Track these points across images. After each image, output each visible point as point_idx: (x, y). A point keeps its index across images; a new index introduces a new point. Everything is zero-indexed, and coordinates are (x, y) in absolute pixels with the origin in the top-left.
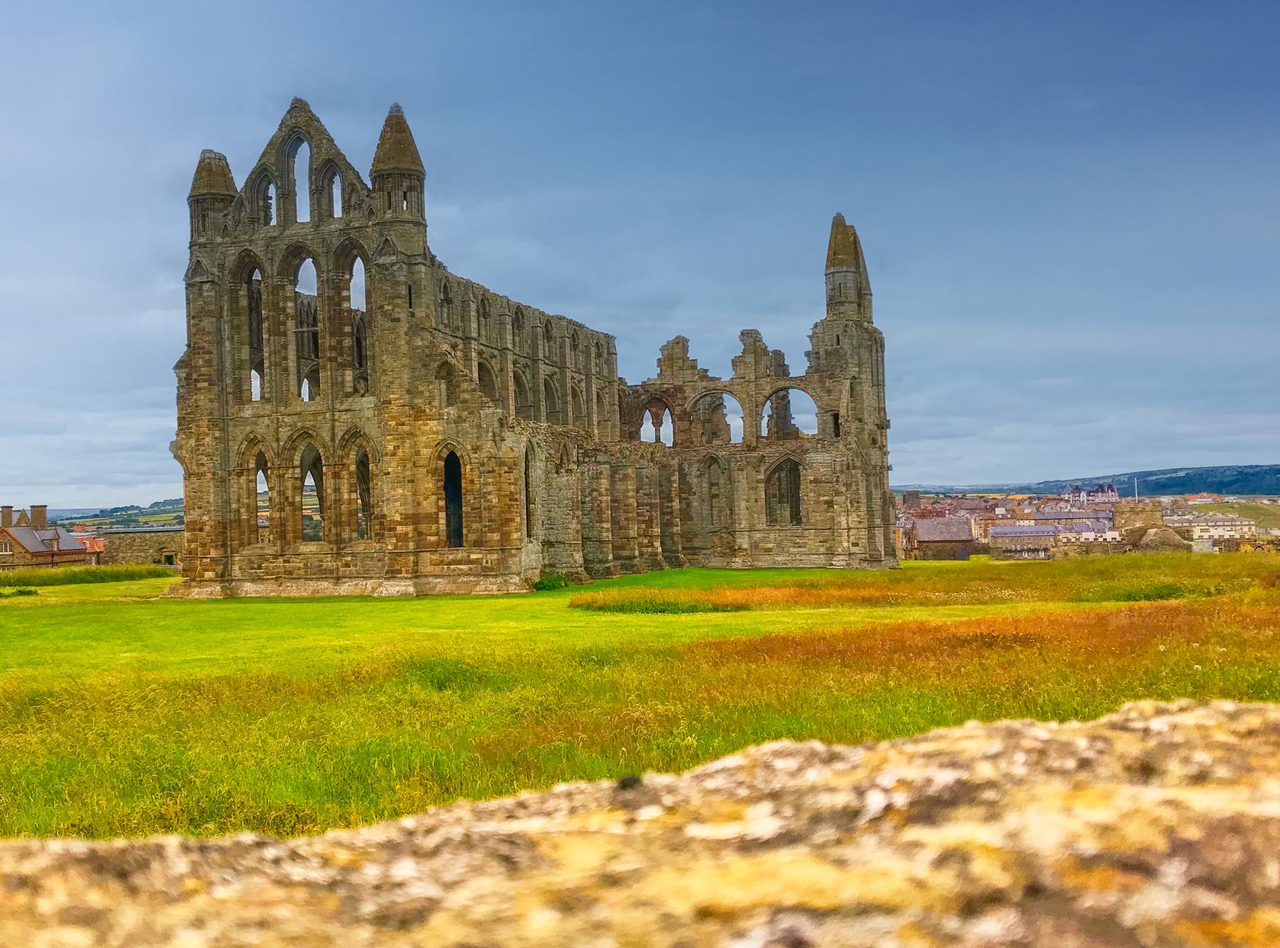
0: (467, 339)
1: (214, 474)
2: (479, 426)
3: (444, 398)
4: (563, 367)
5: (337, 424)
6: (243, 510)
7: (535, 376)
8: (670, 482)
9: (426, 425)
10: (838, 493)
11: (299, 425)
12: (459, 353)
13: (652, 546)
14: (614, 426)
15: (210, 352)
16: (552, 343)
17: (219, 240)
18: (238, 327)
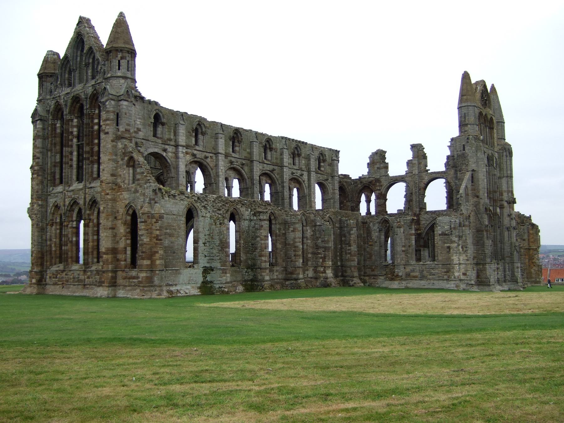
0: (177, 146)
1: (37, 225)
2: (144, 194)
3: (131, 178)
4: (282, 167)
5: (87, 196)
6: (53, 245)
7: (251, 170)
8: (350, 234)
9: (122, 194)
10: (452, 242)
11: (73, 196)
12: (170, 154)
13: (325, 273)
14: (334, 202)
15: (38, 158)
16: (273, 152)
17: (48, 97)
18: (55, 144)
